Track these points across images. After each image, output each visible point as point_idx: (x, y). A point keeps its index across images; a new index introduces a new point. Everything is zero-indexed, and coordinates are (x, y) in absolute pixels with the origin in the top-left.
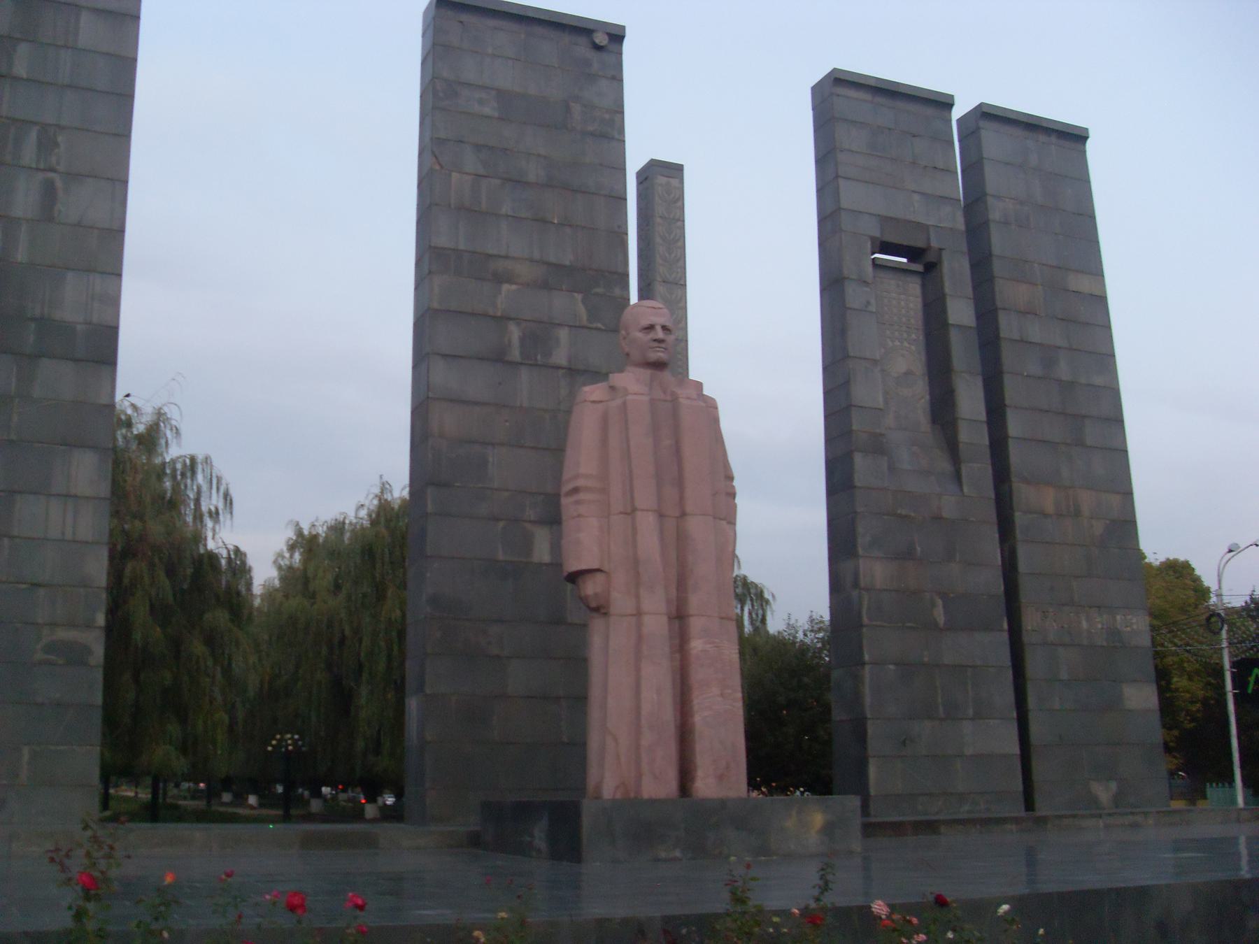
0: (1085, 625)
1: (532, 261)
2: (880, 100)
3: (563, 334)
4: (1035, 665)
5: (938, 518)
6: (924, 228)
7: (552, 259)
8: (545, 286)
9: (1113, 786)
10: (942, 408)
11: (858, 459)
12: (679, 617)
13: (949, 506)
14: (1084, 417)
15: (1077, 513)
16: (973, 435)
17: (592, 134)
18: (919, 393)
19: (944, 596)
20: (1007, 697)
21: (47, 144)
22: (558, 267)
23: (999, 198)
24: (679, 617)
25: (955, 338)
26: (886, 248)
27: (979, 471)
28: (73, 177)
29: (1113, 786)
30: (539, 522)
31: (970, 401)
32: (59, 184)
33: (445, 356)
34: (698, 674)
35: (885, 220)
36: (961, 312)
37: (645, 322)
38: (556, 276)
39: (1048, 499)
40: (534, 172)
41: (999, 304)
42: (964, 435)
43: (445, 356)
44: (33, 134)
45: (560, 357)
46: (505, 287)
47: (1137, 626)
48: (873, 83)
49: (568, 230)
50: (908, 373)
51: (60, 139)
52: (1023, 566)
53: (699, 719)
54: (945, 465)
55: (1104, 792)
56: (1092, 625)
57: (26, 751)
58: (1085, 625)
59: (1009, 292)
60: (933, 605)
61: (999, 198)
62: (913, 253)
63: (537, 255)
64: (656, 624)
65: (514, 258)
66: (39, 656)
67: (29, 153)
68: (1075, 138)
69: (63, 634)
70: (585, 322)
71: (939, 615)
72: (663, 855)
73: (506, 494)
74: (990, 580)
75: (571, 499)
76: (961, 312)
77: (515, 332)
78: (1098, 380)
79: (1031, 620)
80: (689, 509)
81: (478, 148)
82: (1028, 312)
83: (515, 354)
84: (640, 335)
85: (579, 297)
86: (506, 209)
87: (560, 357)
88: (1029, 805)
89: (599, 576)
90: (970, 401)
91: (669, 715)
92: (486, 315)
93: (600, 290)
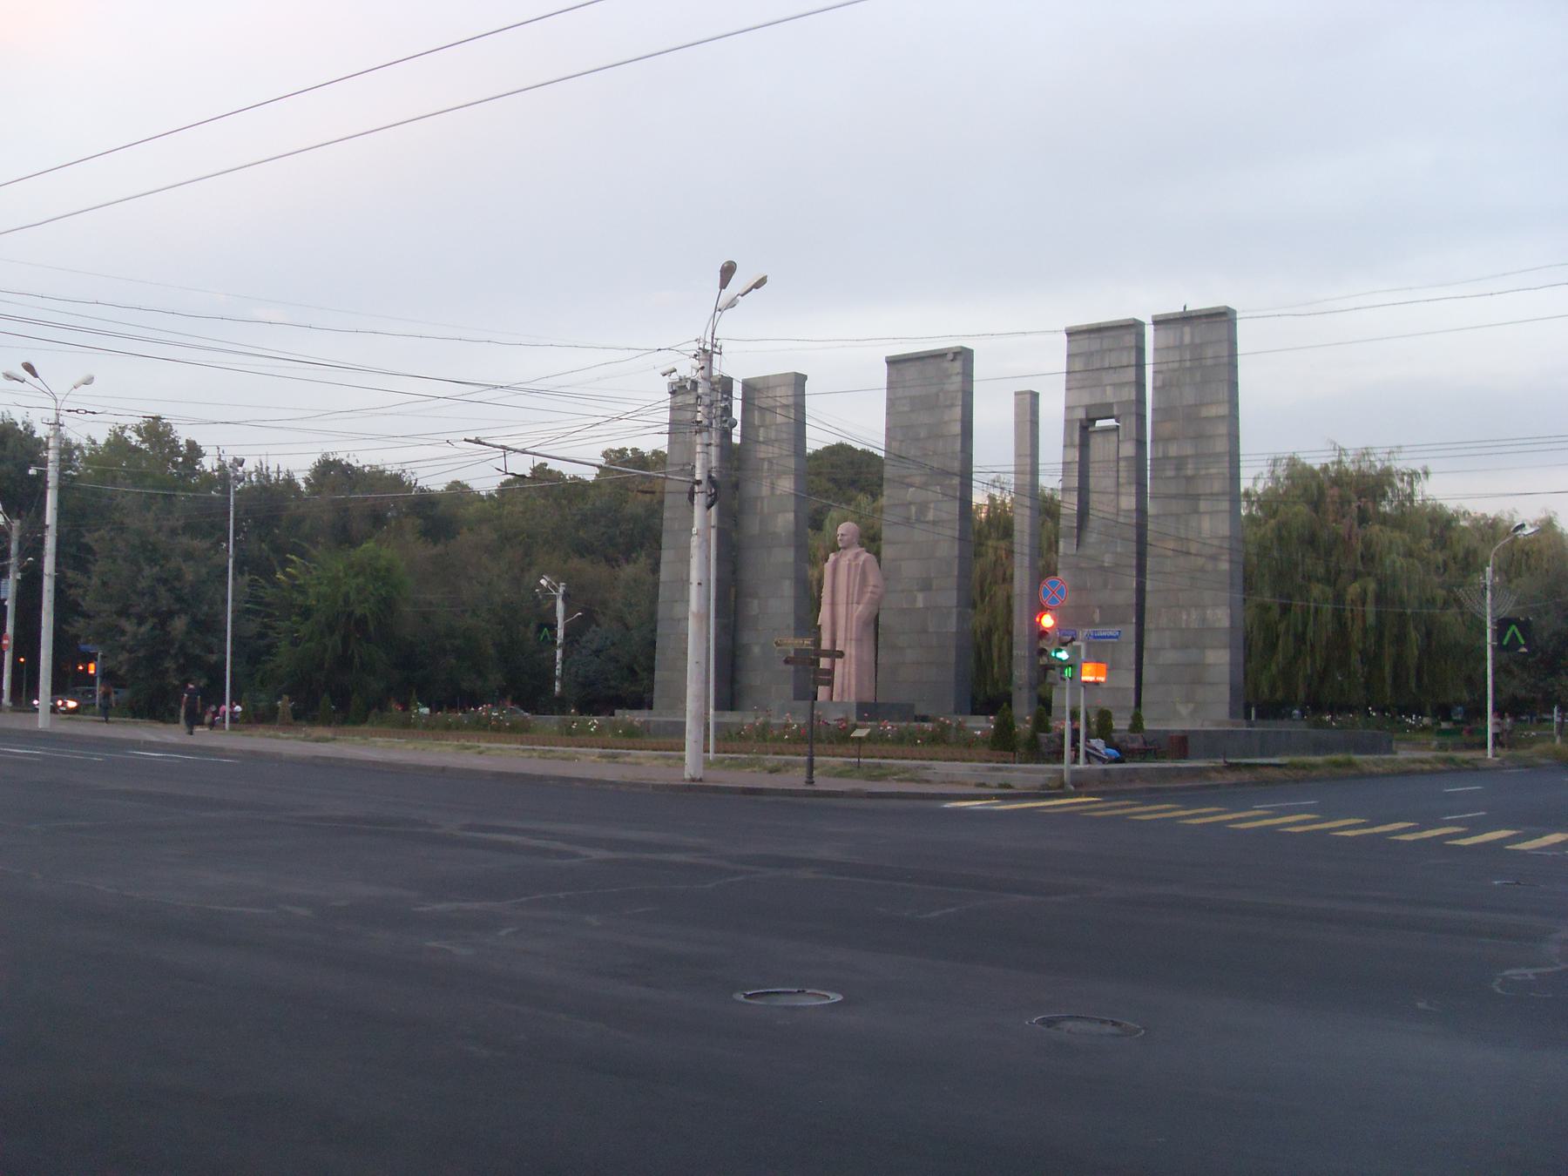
4: (1151, 640)
5: (1101, 568)
9: (1191, 706)
13: (1108, 560)
19: (1100, 607)
28: (779, 477)
29: (1191, 706)
30: (921, 590)
35: (1088, 408)
44: (766, 466)
45: (930, 516)
56: (1190, 618)
71: (1097, 617)
74: (1127, 597)
77: (913, 509)
87: (930, 516)
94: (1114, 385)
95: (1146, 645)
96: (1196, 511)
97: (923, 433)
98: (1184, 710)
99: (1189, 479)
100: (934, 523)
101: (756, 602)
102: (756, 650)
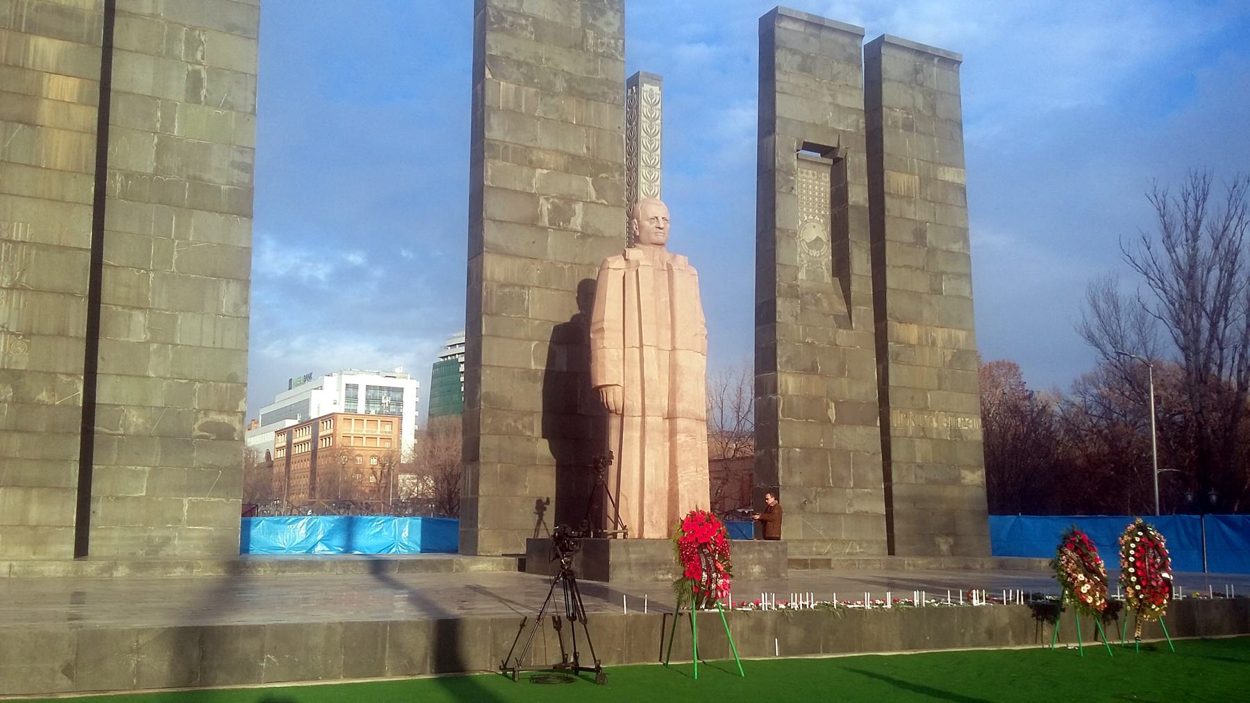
0: (935, 425)
1: (557, 151)
2: (809, 30)
3: (578, 207)
4: (897, 454)
6: (835, 131)
7: (572, 151)
8: (566, 171)
10: (841, 266)
11: (779, 302)
12: (671, 417)
14: (943, 273)
15: (934, 343)
16: (862, 285)
17: (602, 55)
18: (825, 255)
19: (837, 403)
20: (875, 475)
21: (193, 44)
22: (574, 157)
23: (891, 109)
24: (671, 417)
25: (852, 215)
26: (808, 146)
27: (864, 312)
29: (951, 540)
31: (860, 263)
32: (204, 75)
33: (495, 221)
34: (682, 457)
36: (858, 195)
37: (651, 215)
38: (575, 164)
39: (911, 333)
40: (560, 85)
41: (886, 190)
42: (854, 288)
43: (495, 221)
44: (183, 36)
45: (577, 222)
46: (539, 171)
47: (972, 426)
48: (805, 18)
49: (583, 130)
50: (818, 239)
51: (203, 38)
52: (892, 382)
53: (682, 487)
54: (843, 309)
55: (944, 548)
56: (939, 424)
57: (185, 501)
58: (935, 425)
59: (896, 180)
60: (828, 407)
61: (891, 109)
62: (825, 151)
63: (560, 147)
64: (655, 420)
65: (544, 150)
66: (197, 433)
67: (181, 49)
68: (950, 61)
69: (214, 417)
70: (594, 198)
71: (832, 413)
72: (661, 577)
73: (537, 322)
74: (867, 389)
75: (598, 336)
76: (858, 195)
78: (955, 247)
79: (896, 419)
80: (678, 345)
81: (519, 64)
82: (908, 198)
83: (545, 221)
84: (647, 223)
85: (589, 179)
86: (538, 113)
88: (891, 551)
89: (618, 390)
90: (860, 263)
91: (665, 486)
92: (522, 193)
93: (604, 175)
94: (837, 106)
95: (895, 456)
96: (937, 291)
97: (560, 85)
98: (944, 545)
99: (932, 251)
100: (584, 236)
101: (139, 318)
102: (135, 419)
